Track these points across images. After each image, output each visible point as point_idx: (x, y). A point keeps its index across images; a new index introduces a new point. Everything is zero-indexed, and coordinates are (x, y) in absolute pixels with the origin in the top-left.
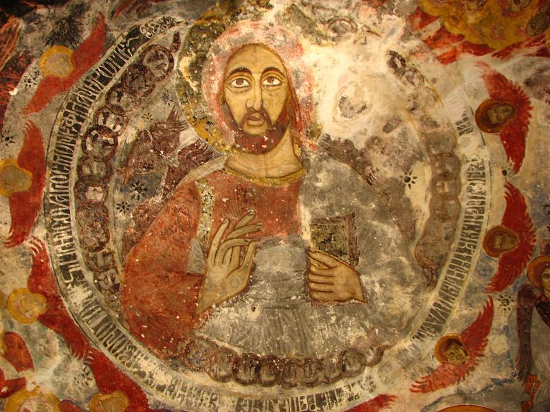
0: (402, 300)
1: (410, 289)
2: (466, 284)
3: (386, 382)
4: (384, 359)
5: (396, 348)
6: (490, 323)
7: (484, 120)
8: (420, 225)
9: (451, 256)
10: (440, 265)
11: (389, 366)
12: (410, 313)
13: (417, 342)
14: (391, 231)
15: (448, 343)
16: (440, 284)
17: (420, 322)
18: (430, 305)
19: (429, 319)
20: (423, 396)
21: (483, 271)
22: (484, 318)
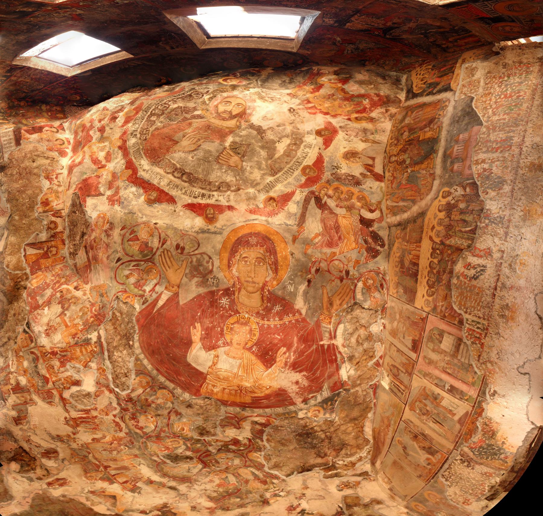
0: (257, 175)
1: (262, 172)
2: (288, 181)
3: (236, 201)
4: (239, 192)
5: (246, 191)
6: (292, 198)
7: (319, 133)
8: (277, 156)
9: (286, 169)
10: (279, 171)
11: (240, 195)
12: (259, 181)
13: (256, 192)
14: (263, 153)
15: (271, 199)
16: (276, 176)
17: (261, 187)
18: (268, 181)
19: (265, 187)
20: (249, 214)
21: (298, 180)
22: (290, 194)
